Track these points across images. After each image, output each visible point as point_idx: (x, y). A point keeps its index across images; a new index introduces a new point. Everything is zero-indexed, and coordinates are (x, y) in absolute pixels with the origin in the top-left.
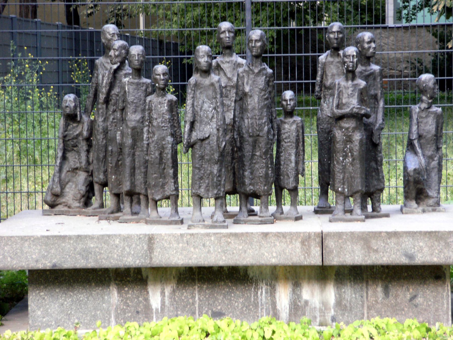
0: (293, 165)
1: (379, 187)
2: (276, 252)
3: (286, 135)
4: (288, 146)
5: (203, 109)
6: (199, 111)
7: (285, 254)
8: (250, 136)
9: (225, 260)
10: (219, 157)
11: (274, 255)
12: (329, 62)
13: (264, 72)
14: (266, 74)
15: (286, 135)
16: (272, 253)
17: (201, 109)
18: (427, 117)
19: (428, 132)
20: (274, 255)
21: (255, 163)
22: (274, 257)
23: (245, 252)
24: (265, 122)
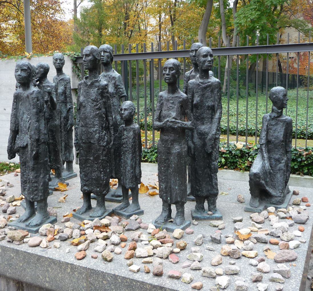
0: (129, 168)
1: (212, 192)
2: (48, 277)
3: (125, 141)
4: (126, 151)
5: (23, 119)
6: (20, 121)
7: (56, 281)
8: (84, 143)
9: (10, 273)
10: (34, 165)
11: (48, 279)
12: (192, 76)
13: (97, 84)
14: (99, 86)
15: (125, 141)
16: (45, 278)
17: (22, 120)
18: (276, 124)
19: (277, 138)
20: (48, 279)
21: (89, 167)
22: (47, 282)
23: (25, 270)
24: (96, 130)
